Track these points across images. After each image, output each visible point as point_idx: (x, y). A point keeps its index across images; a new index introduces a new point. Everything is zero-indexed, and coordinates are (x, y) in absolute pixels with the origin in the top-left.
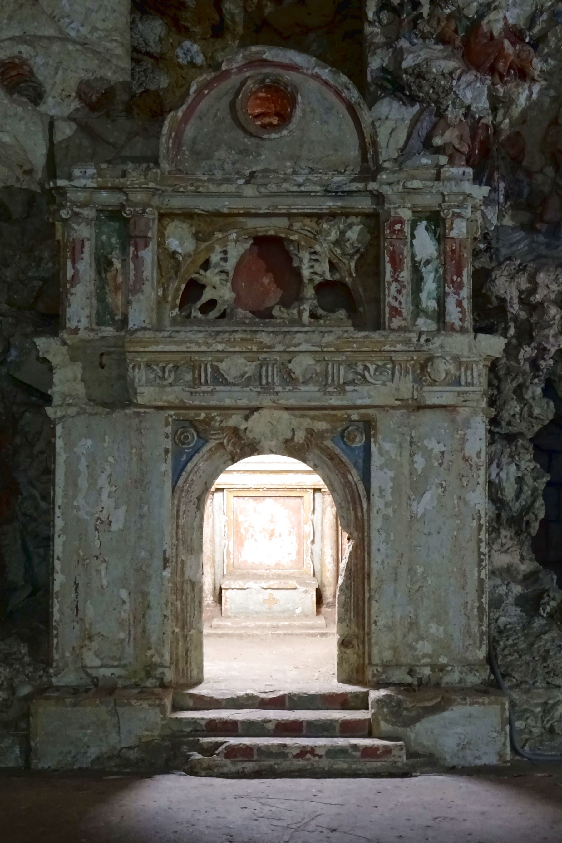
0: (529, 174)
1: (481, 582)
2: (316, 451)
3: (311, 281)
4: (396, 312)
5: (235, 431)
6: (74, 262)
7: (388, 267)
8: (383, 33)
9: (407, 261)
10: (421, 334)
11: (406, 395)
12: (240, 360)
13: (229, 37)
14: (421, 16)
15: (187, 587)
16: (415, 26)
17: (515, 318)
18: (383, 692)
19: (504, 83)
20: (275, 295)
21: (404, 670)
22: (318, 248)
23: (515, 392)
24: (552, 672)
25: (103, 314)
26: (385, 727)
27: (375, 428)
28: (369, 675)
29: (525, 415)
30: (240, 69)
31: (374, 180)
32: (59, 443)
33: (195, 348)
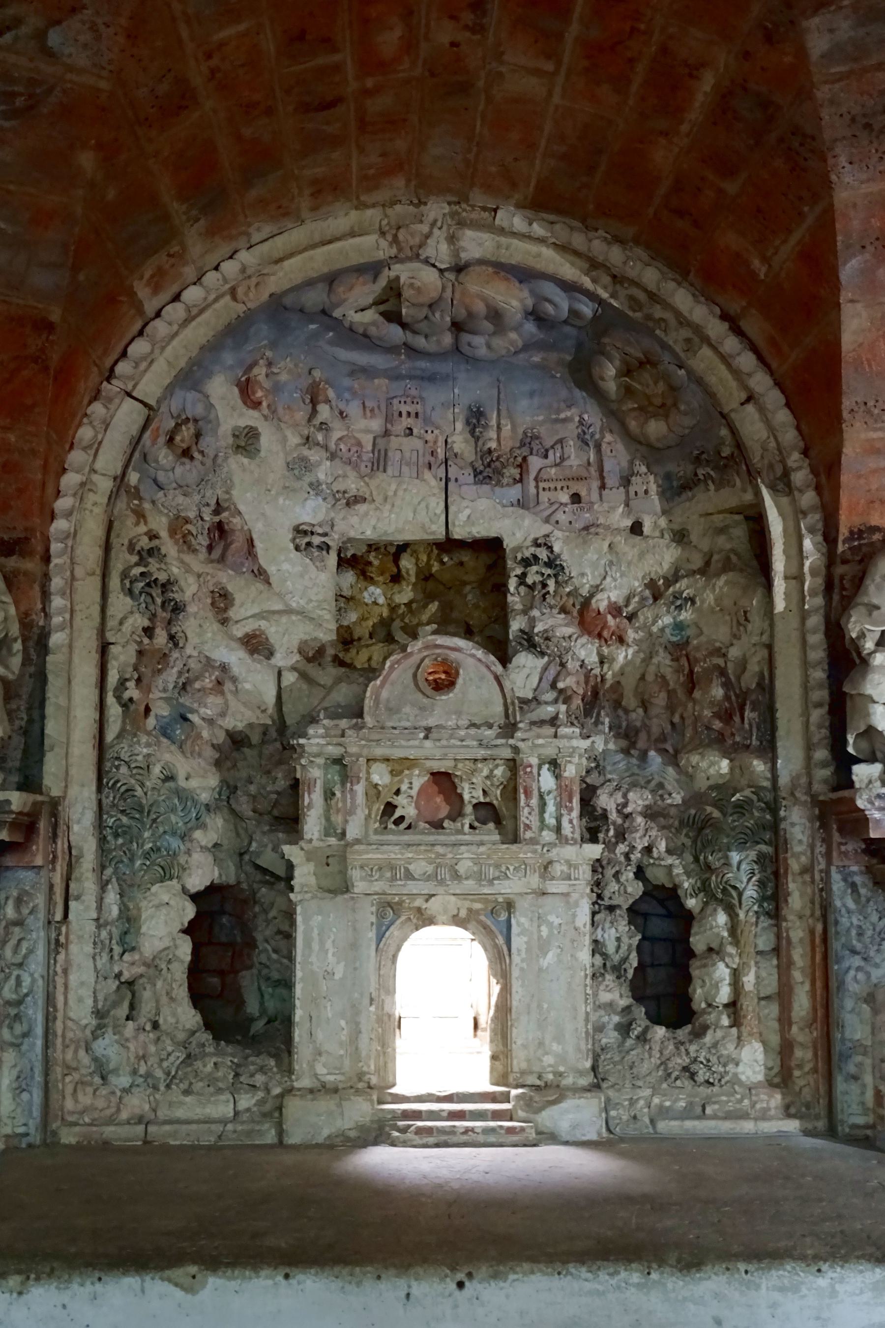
0: (627, 711)
1: (587, 1014)
2: (474, 923)
3: (470, 802)
4: (528, 827)
5: (419, 910)
6: (309, 794)
7: (522, 797)
8: (521, 602)
9: (535, 793)
10: (543, 846)
11: (535, 886)
12: (424, 863)
13: (404, 583)
14: (548, 592)
15: (385, 1018)
16: (544, 599)
17: (614, 823)
18: (520, 1091)
19: (609, 646)
20: (445, 810)
21: (536, 1075)
22: (474, 780)
23: (614, 876)
24: (635, 1077)
25: (329, 830)
26: (521, 1114)
27: (514, 907)
28: (511, 1079)
29: (622, 892)
30: (420, 650)
31: (512, 737)
32: (299, 919)
33: (393, 856)
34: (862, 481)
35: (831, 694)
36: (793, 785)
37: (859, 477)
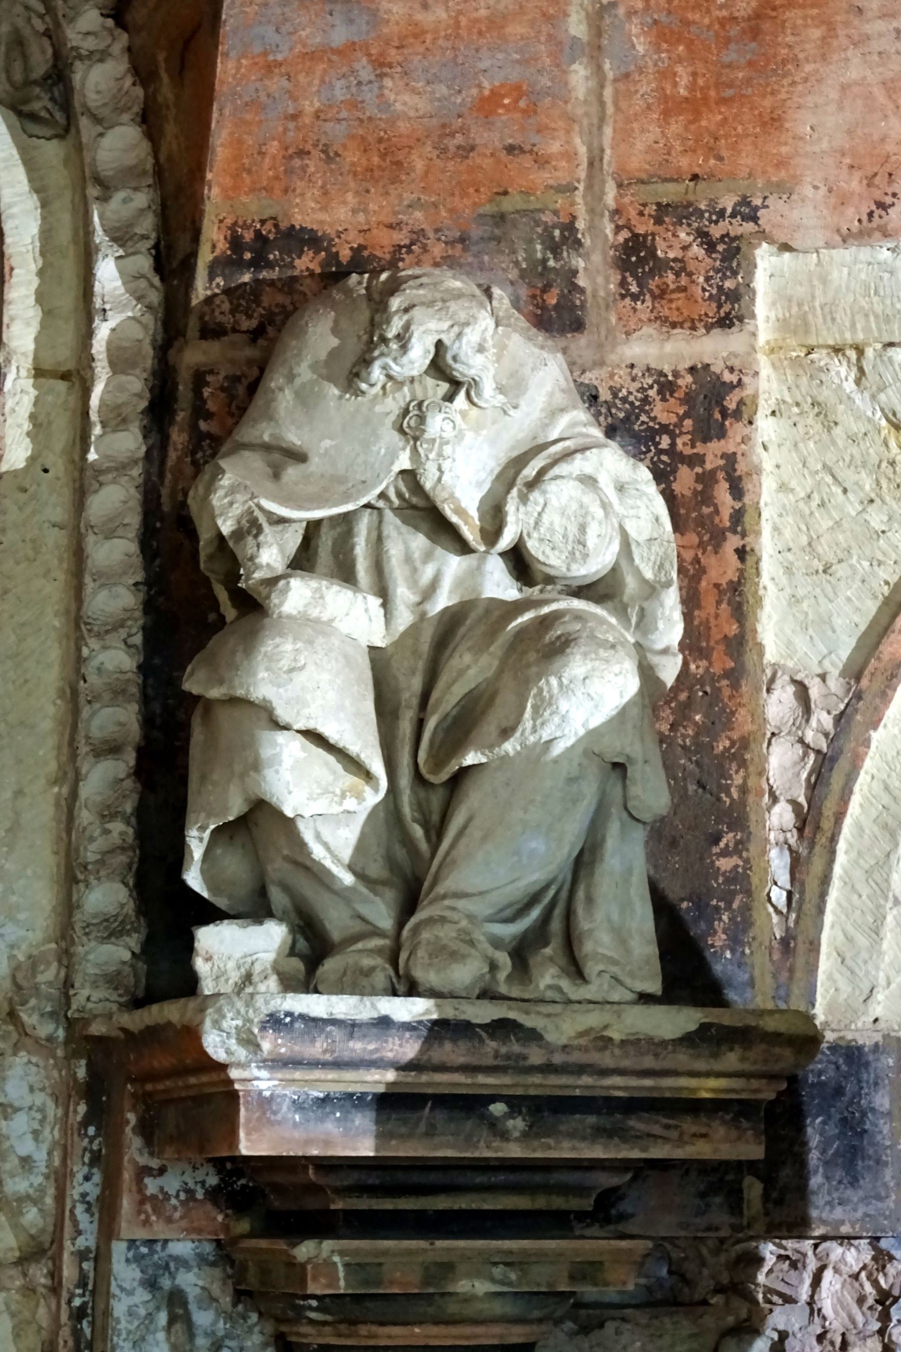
34: (277, 84)
35: (147, 721)
36: (18, 987)
37: (270, 68)
